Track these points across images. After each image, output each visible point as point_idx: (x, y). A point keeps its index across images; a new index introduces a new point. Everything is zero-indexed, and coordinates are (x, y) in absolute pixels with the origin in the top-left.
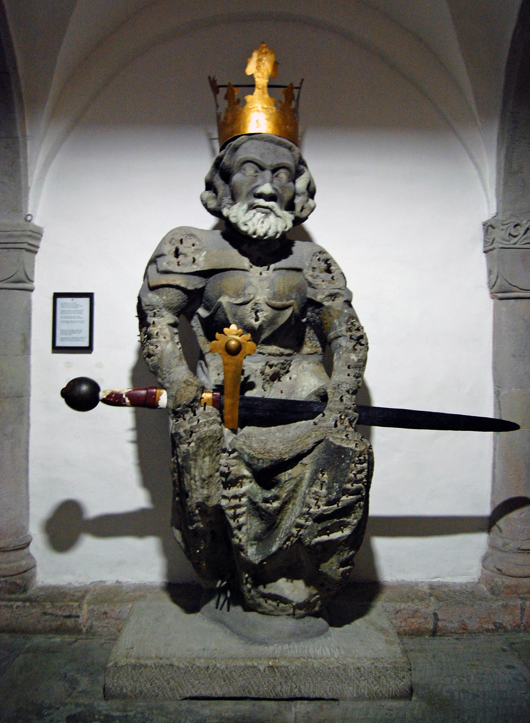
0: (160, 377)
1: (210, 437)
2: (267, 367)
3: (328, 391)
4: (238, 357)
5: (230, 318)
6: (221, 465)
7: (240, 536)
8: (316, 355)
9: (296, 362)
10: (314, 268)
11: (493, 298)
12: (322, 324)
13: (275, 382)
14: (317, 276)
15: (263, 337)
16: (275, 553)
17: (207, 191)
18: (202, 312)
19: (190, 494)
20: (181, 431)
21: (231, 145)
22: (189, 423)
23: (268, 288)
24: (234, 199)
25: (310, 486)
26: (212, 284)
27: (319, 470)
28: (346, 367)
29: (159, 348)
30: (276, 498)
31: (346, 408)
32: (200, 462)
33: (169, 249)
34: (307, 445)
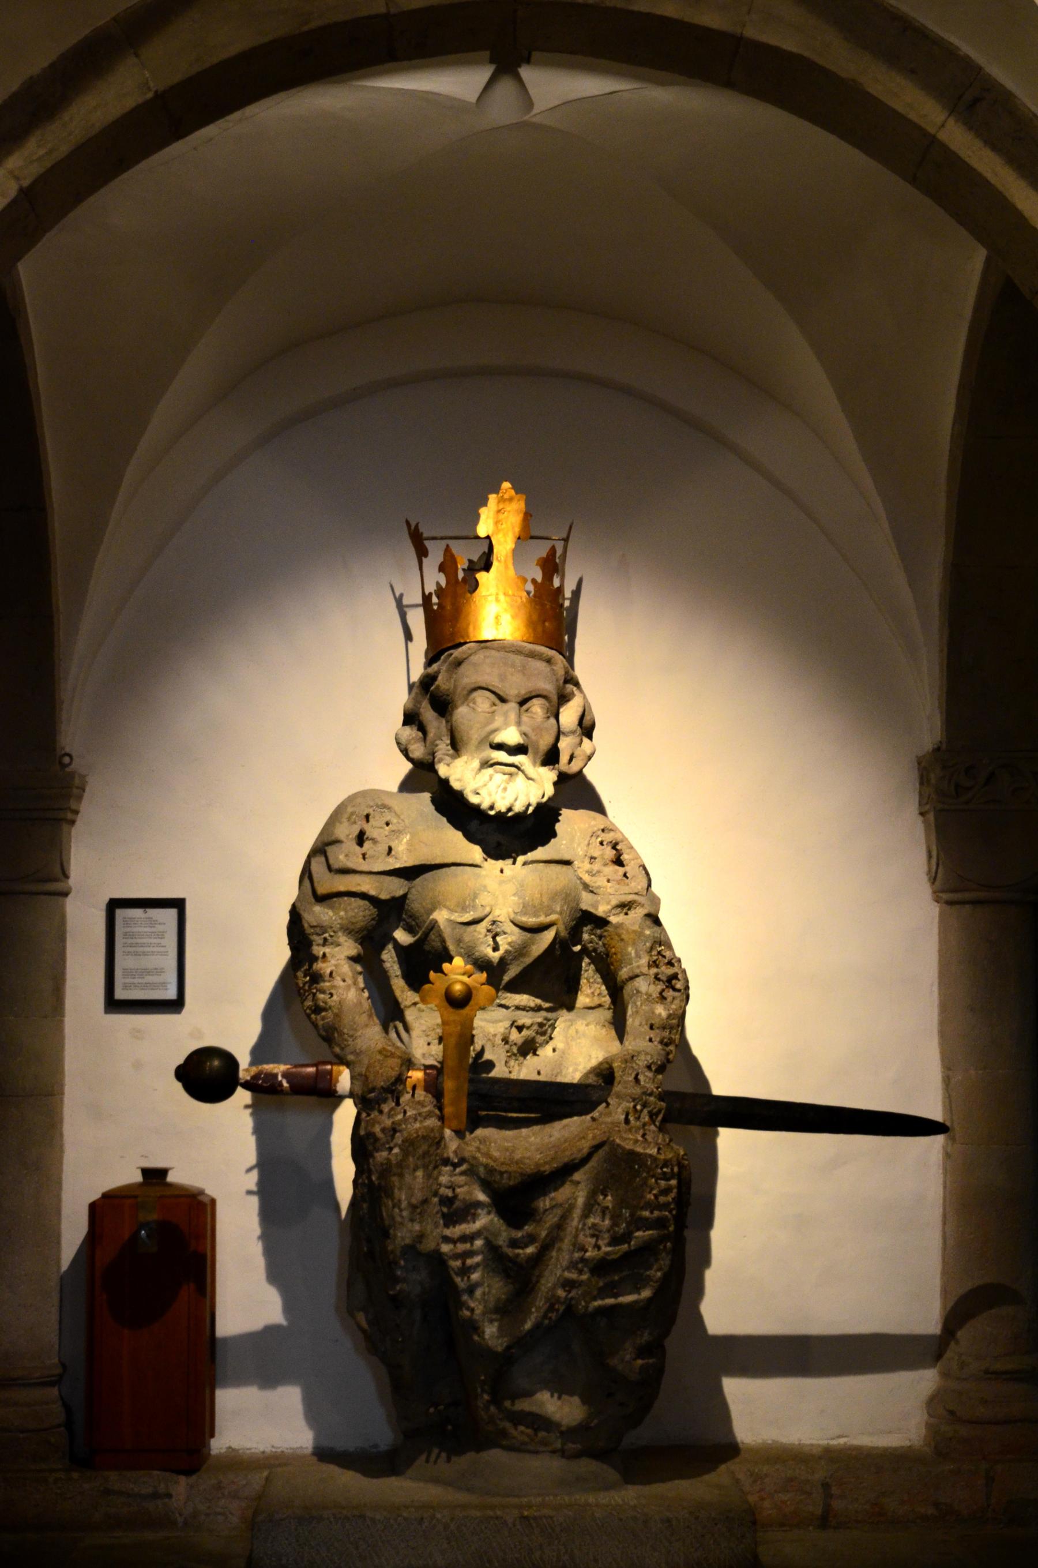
0: (339, 1045)
1: (424, 1137)
2: (514, 1030)
3: (615, 1065)
4: (466, 1011)
5: (451, 947)
6: (440, 1185)
7: (472, 1305)
8: (601, 1009)
9: (565, 1021)
10: (593, 858)
11: (937, 902)
12: (607, 955)
13: (528, 1057)
14: (599, 872)
15: (506, 978)
16: (531, 1332)
17: (407, 728)
18: (401, 936)
19: (391, 1231)
20: (377, 1129)
21: (451, 654)
22: (389, 1117)
23: (514, 895)
24: (456, 746)
25: (585, 1215)
26: (419, 889)
27: (599, 1188)
28: (647, 1028)
29: (335, 997)
30: (531, 1239)
31: (644, 1093)
32: (408, 1178)
33: (346, 831)
34: (580, 1150)
